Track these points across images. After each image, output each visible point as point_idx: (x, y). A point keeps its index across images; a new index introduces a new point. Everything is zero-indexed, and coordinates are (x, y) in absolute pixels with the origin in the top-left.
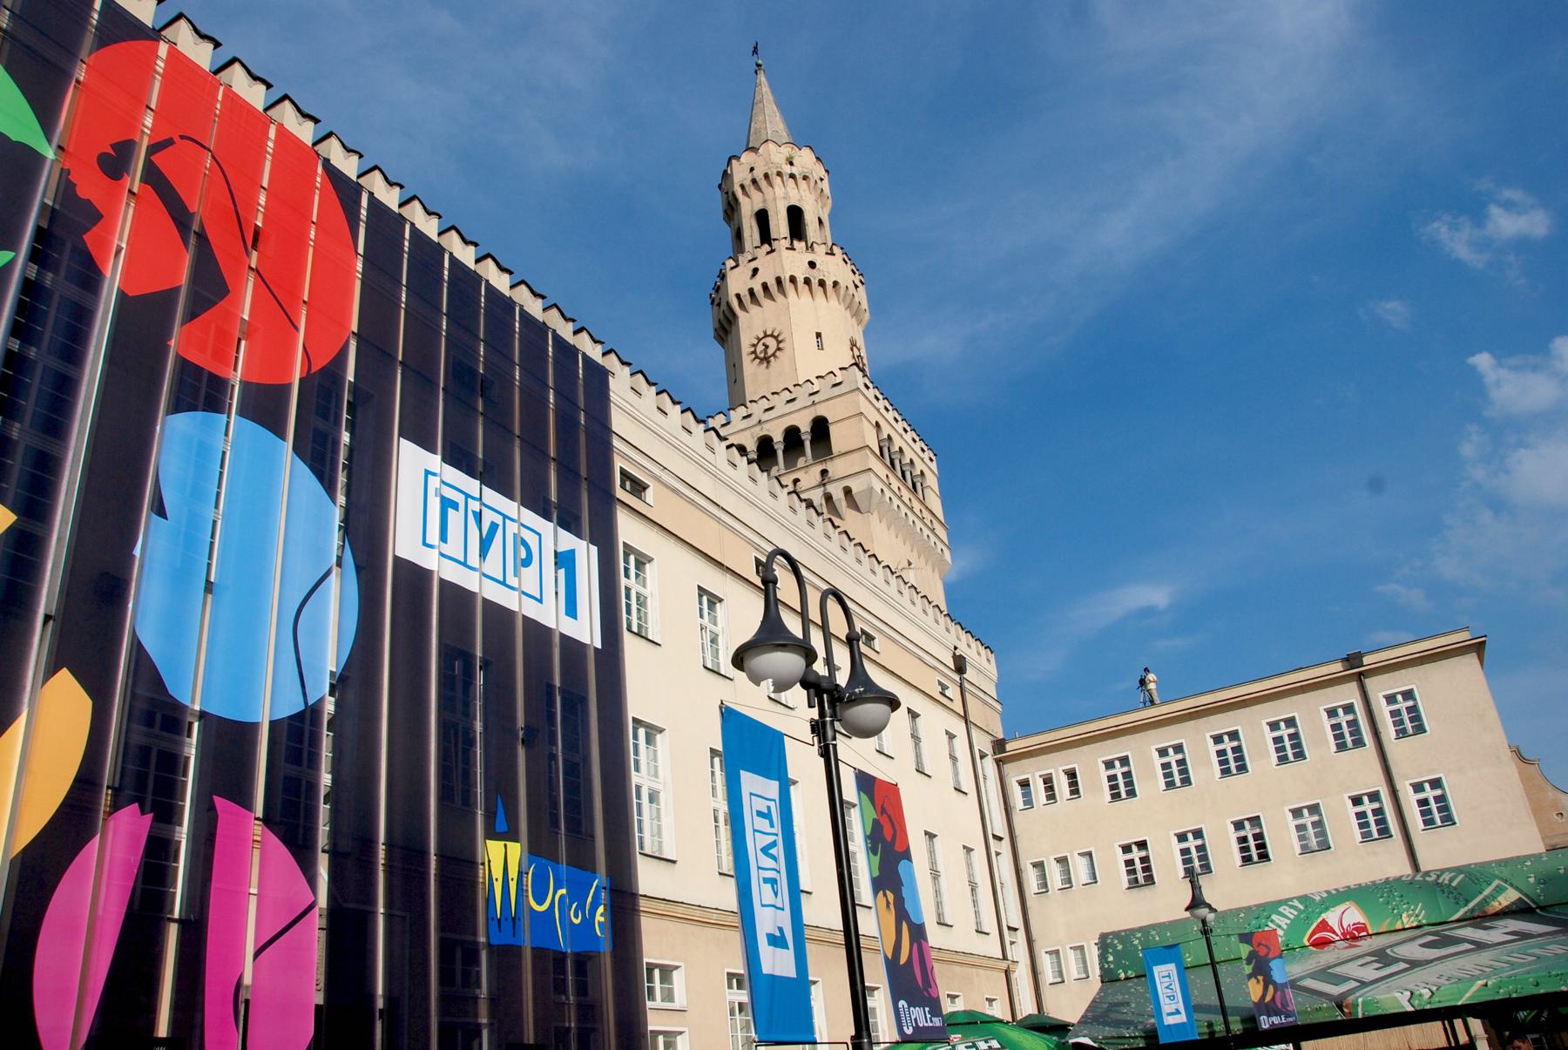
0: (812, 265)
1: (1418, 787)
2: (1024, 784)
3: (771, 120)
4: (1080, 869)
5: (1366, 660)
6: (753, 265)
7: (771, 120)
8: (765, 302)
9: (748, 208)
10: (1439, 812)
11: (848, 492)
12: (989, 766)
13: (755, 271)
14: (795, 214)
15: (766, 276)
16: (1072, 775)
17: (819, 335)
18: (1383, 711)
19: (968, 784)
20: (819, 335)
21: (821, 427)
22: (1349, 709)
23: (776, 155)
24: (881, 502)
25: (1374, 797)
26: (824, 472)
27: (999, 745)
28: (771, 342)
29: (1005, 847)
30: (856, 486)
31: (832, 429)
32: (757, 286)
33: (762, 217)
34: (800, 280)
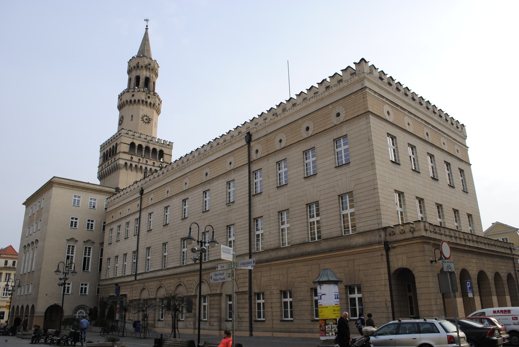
0: (149, 97)
6: (134, 93)
13: (133, 95)
15: (136, 98)
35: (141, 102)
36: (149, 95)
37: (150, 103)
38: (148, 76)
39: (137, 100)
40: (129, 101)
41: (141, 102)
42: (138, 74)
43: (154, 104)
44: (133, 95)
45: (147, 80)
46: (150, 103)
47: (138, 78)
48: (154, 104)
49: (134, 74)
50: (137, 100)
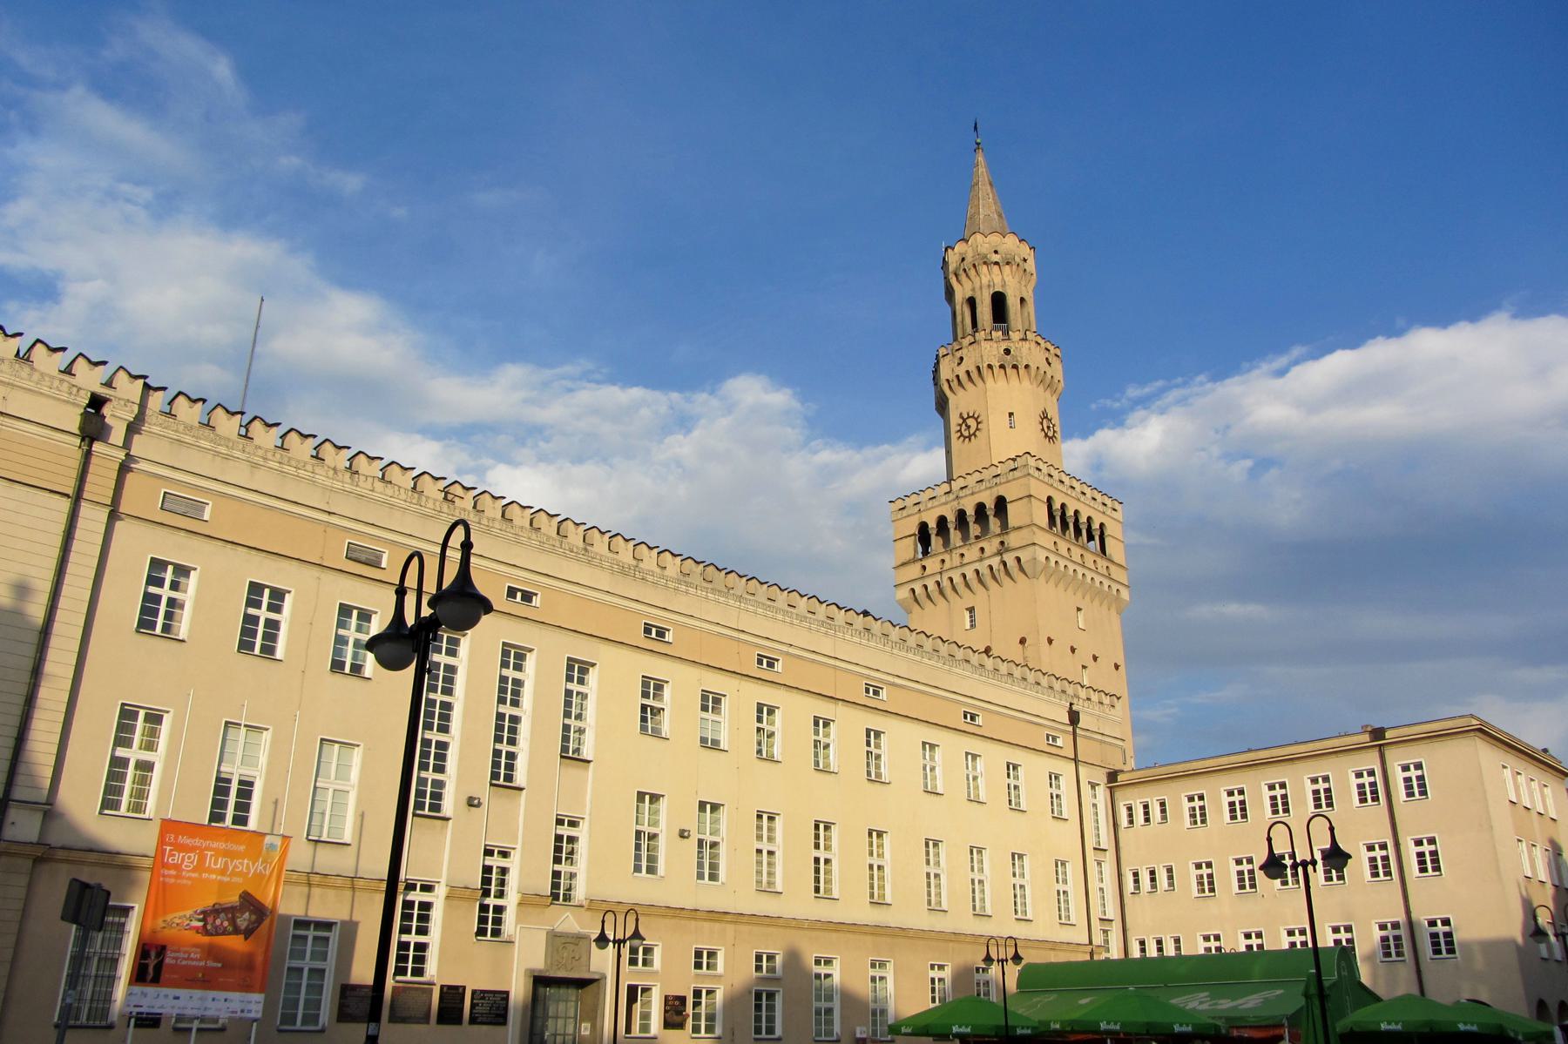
0: (1007, 352)
1: (1419, 843)
2: (1130, 809)
3: (986, 205)
4: (1162, 877)
5: (1388, 735)
7: (986, 205)
8: (968, 385)
9: (961, 294)
10: (1430, 862)
12: (1102, 792)
14: (999, 301)
16: (1163, 804)
17: (1011, 414)
18: (1398, 777)
19: (1068, 807)
21: (1001, 503)
22: (1371, 773)
23: (982, 243)
24: (1046, 567)
25: (1383, 847)
26: (1002, 543)
27: (1112, 776)
28: (971, 422)
29: (1110, 857)
30: (1025, 556)
31: (1009, 506)
32: (961, 371)
33: (972, 302)
34: (996, 364)
41: (985, 371)
42: (969, 294)
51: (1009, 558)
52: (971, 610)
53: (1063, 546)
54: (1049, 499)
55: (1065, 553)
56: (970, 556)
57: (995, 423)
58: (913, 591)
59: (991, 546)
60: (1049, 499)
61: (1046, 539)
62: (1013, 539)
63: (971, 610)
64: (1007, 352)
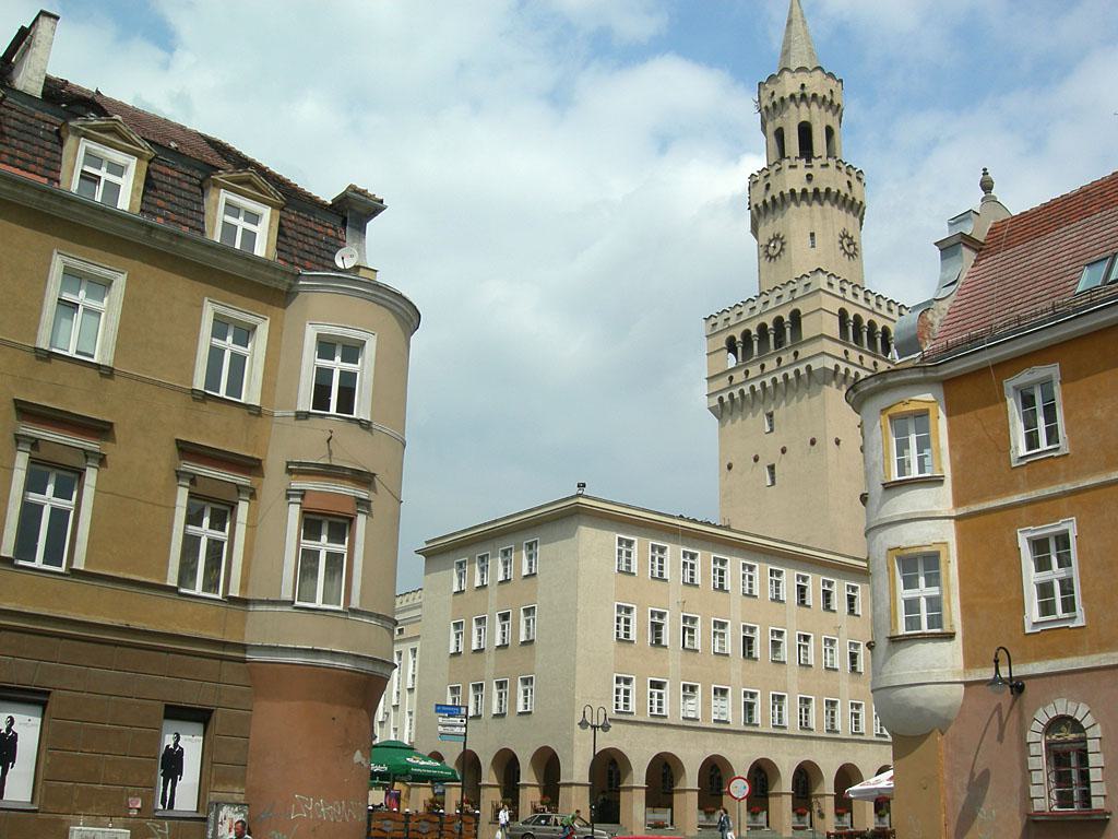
11: (809, 368)
13: (768, 186)
17: (812, 235)
20: (812, 235)
21: (796, 317)
31: (803, 321)
34: (798, 191)
35: (788, 198)
36: (809, 171)
37: (816, 191)
38: (804, 118)
39: (777, 196)
40: (760, 205)
41: (788, 198)
43: (828, 190)
44: (768, 186)
45: (805, 131)
46: (816, 191)
47: (780, 134)
48: (828, 190)
49: (771, 128)
50: (777, 196)
51: (802, 369)
52: (770, 416)
53: (854, 355)
54: (843, 314)
55: (857, 362)
56: (774, 367)
57: (798, 246)
58: (721, 399)
59: (787, 358)
60: (843, 314)
61: (838, 350)
62: (804, 352)
63: (770, 416)
64: (809, 177)
